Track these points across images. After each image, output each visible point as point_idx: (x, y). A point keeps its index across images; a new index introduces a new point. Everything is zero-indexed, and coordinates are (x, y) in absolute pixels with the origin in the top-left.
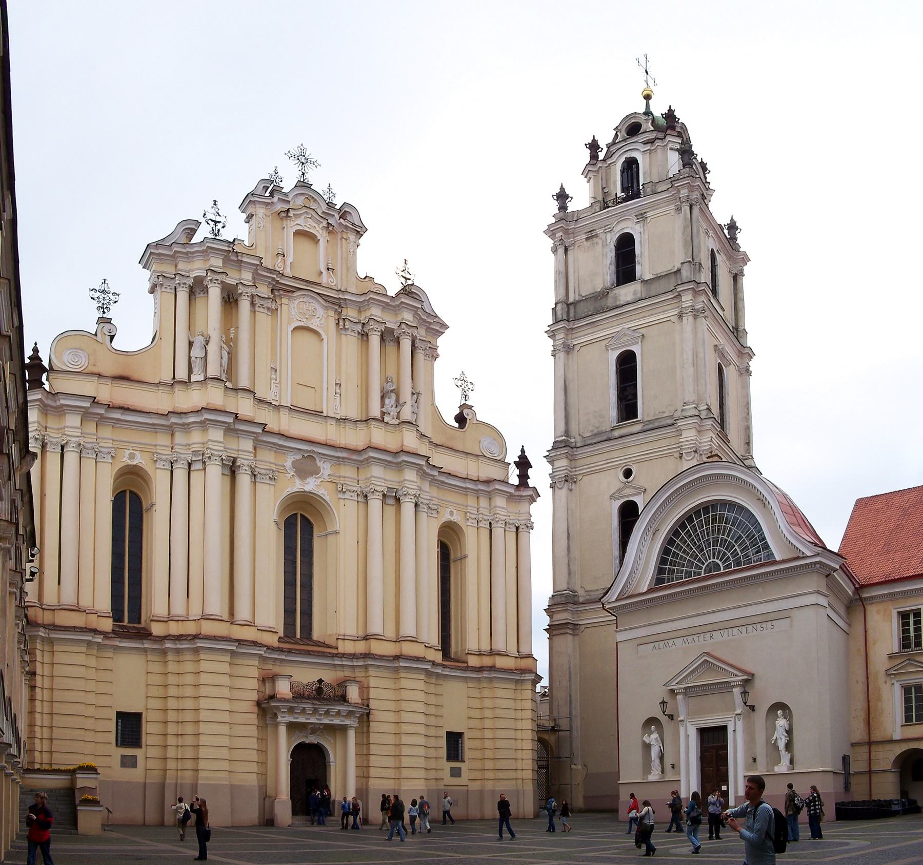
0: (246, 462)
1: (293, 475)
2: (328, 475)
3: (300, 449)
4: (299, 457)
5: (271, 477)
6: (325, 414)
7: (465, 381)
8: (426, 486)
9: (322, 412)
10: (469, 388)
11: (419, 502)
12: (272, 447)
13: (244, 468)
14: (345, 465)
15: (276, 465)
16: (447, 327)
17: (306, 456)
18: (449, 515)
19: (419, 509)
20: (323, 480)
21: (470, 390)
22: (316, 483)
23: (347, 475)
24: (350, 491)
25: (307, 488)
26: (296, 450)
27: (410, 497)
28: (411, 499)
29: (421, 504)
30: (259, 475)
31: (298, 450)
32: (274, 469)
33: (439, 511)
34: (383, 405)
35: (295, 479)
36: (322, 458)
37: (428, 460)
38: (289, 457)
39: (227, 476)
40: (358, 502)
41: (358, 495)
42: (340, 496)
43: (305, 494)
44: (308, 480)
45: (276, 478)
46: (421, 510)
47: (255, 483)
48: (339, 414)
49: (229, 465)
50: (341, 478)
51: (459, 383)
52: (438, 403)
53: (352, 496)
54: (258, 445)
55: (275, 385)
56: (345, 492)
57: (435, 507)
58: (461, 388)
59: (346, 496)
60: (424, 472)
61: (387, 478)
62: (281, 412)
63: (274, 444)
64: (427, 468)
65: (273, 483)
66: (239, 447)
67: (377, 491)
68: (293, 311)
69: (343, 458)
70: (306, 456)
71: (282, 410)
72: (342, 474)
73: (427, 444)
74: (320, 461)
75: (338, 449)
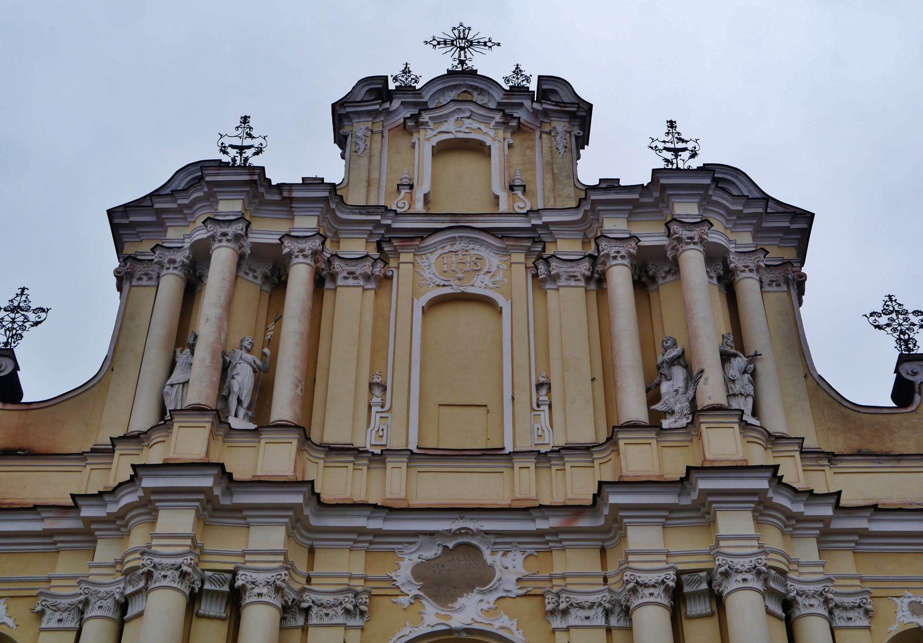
0: (261, 577)
1: (416, 597)
2: (518, 580)
3: (431, 534)
4: (431, 552)
5: (350, 606)
6: (509, 448)
7: (898, 313)
8: (807, 550)
9: (503, 449)
10: (914, 325)
11: (788, 592)
12: (355, 541)
13: (256, 590)
14: (564, 549)
15: (366, 580)
16: (809, 217)
17: (451, 546)
18: (908, 613)
19: (797, 613)
20: (504, 594)
21: (916, 328)
22: (484, 606)
23: (571, 570)
24: (581, 607)
25: (458, 621)
26: (421, 539)
27: (740, 577)
28: (745, 580)
29: (798, 598)
30: (315, 609)
31: (427, 538)
32: (359, 589)
33: (869, 607)
34: (653, 395)
35: (423, 606)
36: (495, 543)
37: (775, 474)
38: (406, 557)
39: (219, 622)
40: (609, 630)
41: (607, 613)
42: (557, 623)
43: (456, 636)
44: (461, 601)
45: (363, 608)
46: (804, 611)
47: (305, 629)
48: (548, 444)
49: (222, 593)
50: (555, 582)
51: (883, 320)
52: (823, 367)
53: (587, 618)
54: (315, 543)
55: (379, 415)
56: (565, 612)
57: (857, 600)
58: (888, 329)
59: (573, 619)
60: (790, 516)
61: (672, 549)
62: (389, 465)
63: (361, 531)
64: (793, 502)
65: (357, 622)
66: (247, 547)
67: (646, 586)
68: (428, 271)
69: (554, 532)
70: (451, 546)
71: (391, 462)
72: (558, 570)
73: (797, 454)
74: (493, 552)
75: (535, 513)
